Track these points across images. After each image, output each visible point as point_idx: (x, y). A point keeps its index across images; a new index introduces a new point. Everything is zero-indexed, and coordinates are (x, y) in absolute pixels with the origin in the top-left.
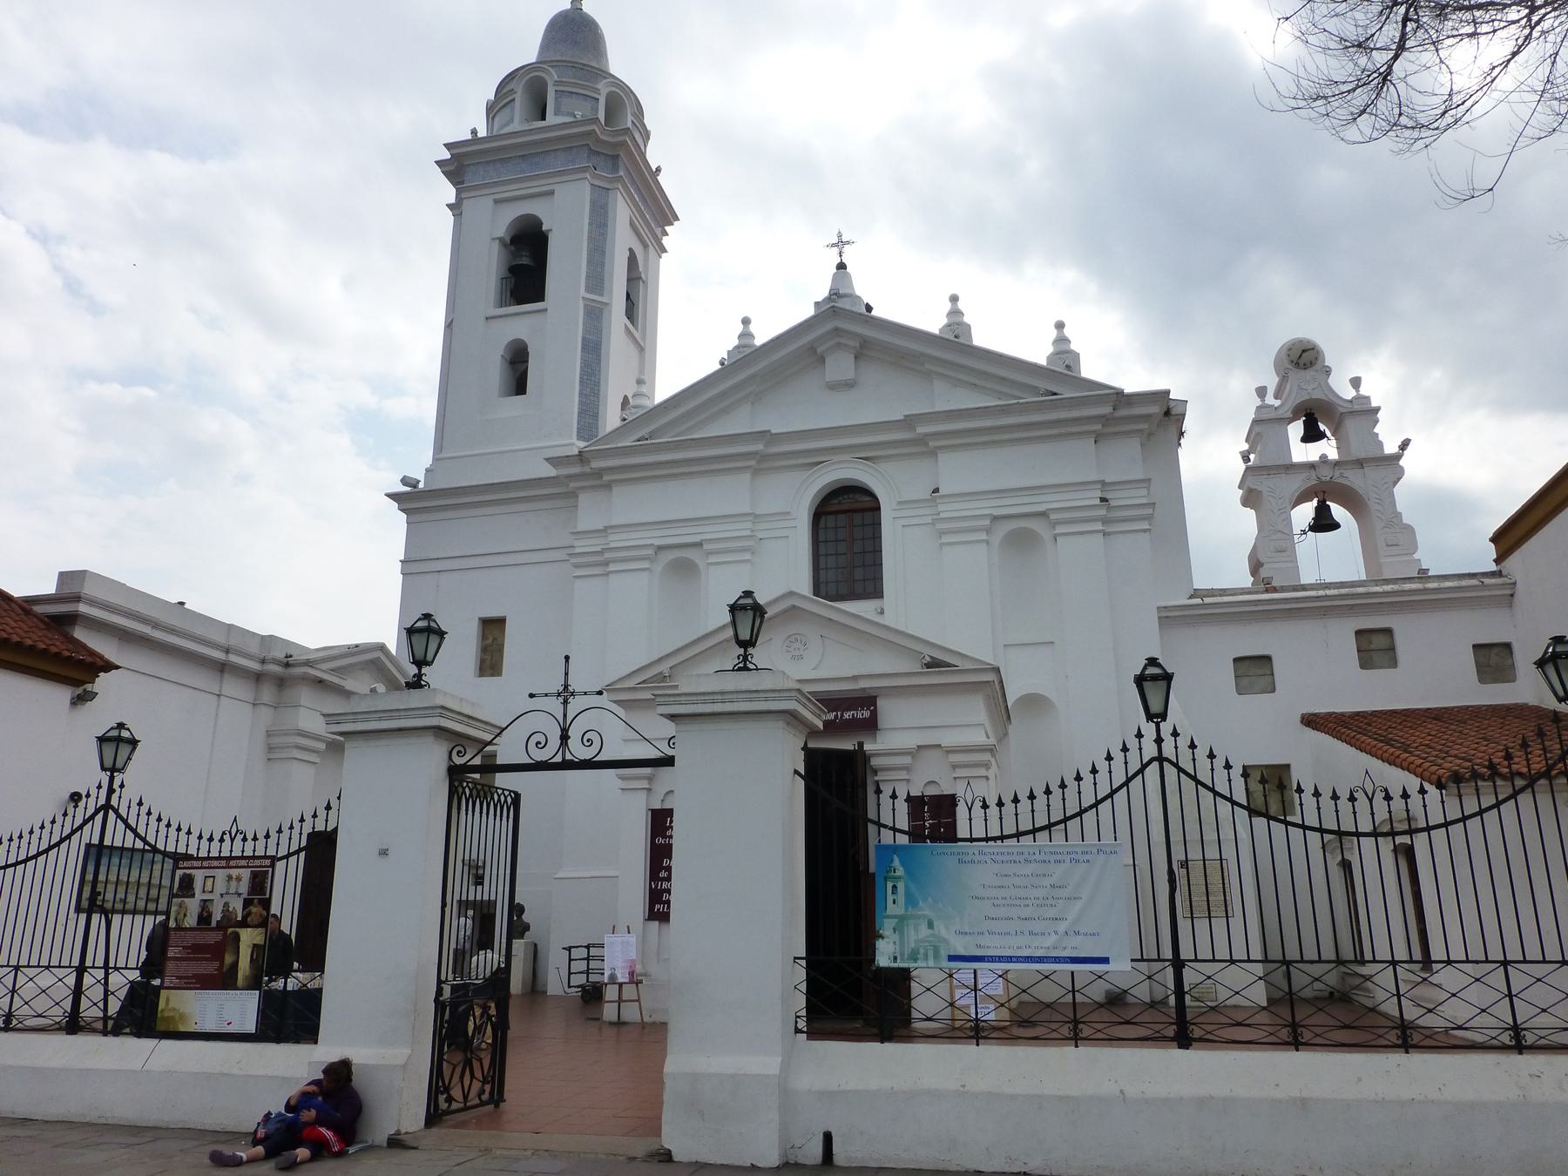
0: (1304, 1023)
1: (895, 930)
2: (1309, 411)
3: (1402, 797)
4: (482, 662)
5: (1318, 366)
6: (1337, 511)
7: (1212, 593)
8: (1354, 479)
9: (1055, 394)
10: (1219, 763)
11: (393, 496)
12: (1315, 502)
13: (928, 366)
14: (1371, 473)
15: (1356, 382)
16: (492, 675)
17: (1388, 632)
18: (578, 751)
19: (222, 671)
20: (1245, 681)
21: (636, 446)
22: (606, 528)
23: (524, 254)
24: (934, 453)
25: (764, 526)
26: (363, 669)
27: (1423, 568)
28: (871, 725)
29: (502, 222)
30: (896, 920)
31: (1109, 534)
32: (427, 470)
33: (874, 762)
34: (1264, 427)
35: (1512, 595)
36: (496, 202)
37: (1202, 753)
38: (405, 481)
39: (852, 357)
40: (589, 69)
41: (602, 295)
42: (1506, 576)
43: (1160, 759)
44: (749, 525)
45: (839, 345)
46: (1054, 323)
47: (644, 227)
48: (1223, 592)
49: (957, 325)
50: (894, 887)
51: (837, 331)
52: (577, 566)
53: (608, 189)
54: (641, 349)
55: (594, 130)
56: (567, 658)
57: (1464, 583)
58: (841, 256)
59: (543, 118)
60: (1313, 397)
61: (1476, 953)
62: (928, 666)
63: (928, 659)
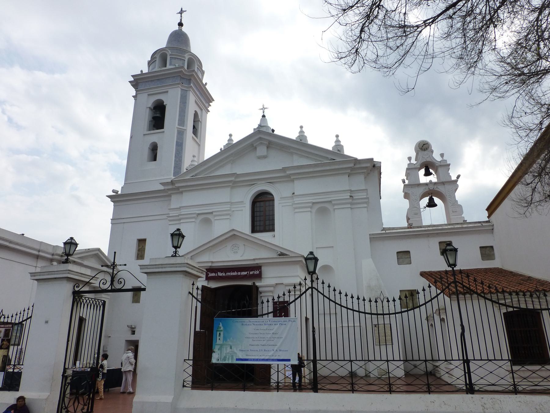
0: (356, 383)
1: (219, 349)
2: (426, 165)
3: (393, 301)
4: (138, 254)
5: (429, 149)
6: (437, 200)
7: (389, 229)
8: (441, 189)
9: (334, 160)
10: (332, 289)
11: (108, 196)
12: (428, 198)
13: (292, 150)
14: (448, 187)
15: (442, 155)
16: (141, 259)
18: (118, 286)
19: (37, 258)
20: (401, 260)
21: (191, 178)
22: (180, 207)
23: (158, 112)
24: (293, 181)
25: (234, 206)
26: (92, 257)
27: (465, 220)
28: (259, 276)
29: (150, 102)
30: (219, 346)
31: (353, 208)
32: (122, 187)
33: (260, 289)
34: (411, 170)
35: (493, 229)
36: (149, 95)
37: (326, 285)
38: (113, 191)
39: (266, 148)
40: (182, 50)
41: (183, 126)
42: (491, 223)
43: (312, 288)
44: (229, 206)
46: (231, 133)
47: (201, 104)
48: (393, 229)
49: (302, 136)
50: (220, 334)
51: (260, 139)
52: (170, 221)
53: (187, 91)
54: (199, 145)
55: (182, 71)
56: (115, 253)
57: (476, 225)
58: (264, 113)
59: (165, 65)
60: (427, 160)
61: (341, 358)
62: (279, 255)
63: (279, 253)
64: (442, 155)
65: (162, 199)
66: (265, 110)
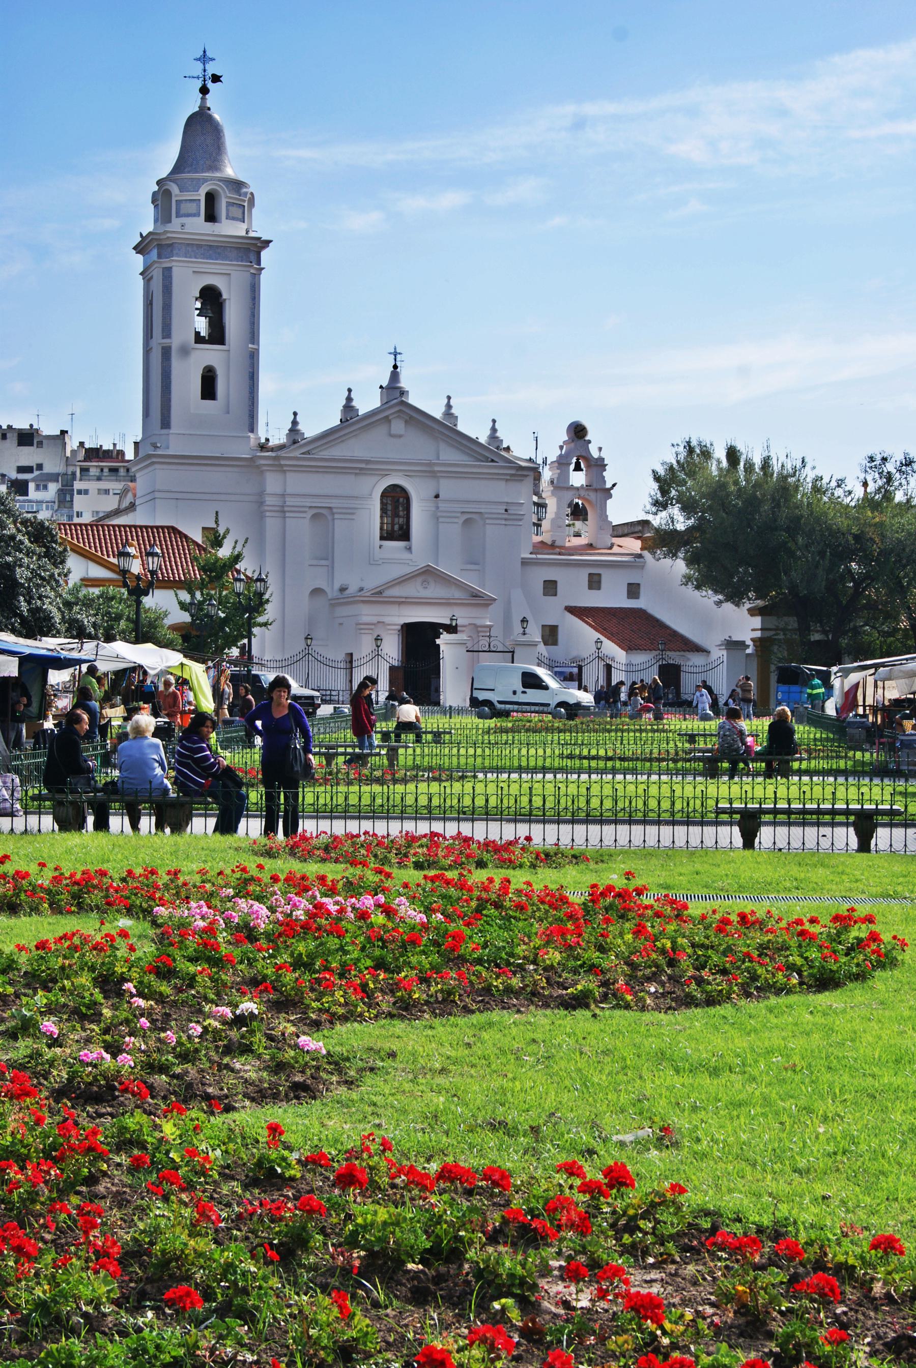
9: (493, 461)
15: (600, 449)
17: (599, 575)
45: (399, 417)
64: (600, 449)
65: (235, 469)
66: (398, 357)
